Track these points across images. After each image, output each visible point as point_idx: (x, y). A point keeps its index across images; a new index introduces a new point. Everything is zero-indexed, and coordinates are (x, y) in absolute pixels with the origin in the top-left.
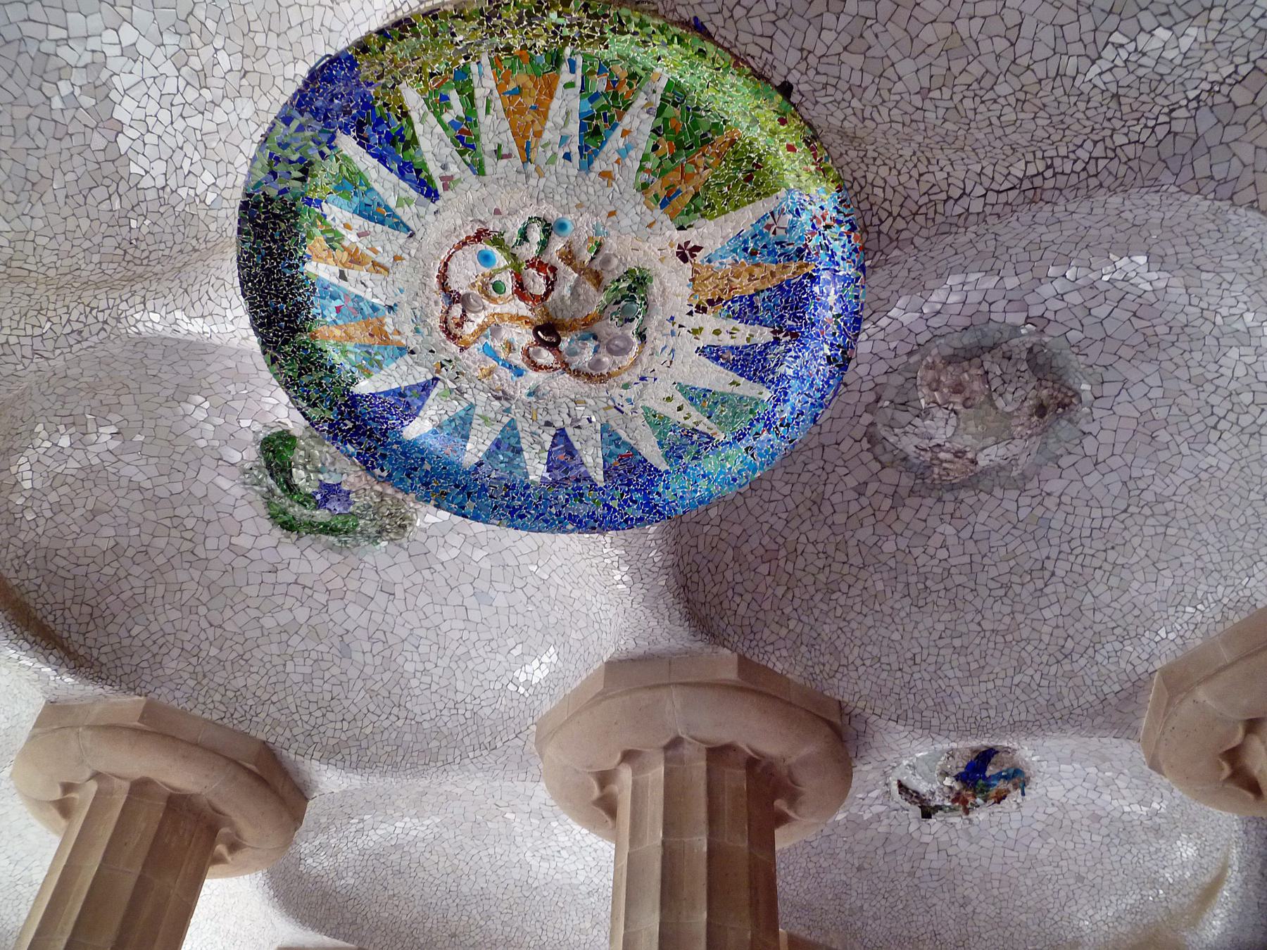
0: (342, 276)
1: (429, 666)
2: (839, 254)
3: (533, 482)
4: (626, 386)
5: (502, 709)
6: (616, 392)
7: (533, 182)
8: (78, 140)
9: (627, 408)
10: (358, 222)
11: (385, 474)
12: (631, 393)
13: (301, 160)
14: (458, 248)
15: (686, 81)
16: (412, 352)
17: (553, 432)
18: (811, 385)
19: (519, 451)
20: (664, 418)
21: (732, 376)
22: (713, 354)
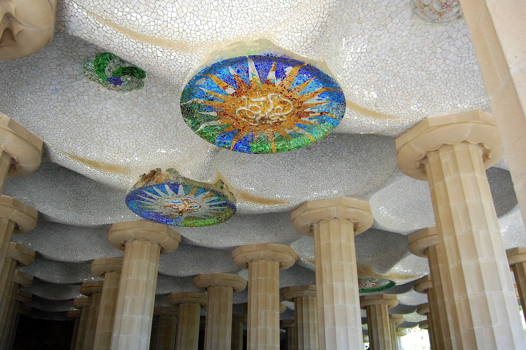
1: (24, 74)
5: (8, 100)
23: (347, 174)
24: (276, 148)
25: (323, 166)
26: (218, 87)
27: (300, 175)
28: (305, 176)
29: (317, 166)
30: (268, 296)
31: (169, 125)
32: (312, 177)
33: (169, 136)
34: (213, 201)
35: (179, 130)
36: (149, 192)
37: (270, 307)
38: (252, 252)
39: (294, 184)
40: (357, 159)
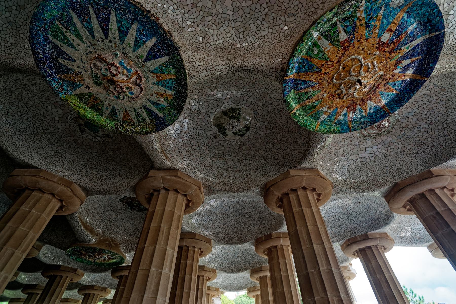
0: (165, 91)
2: (53, 83)
3: (113, 11)
4: (91, 52)
6: (93, 51)
7: (124, 106)
9: (89, 44)
10: (160, 103)
11: (160, 30)
12: (89, 50)
13: (169, 115)
14: (138, 96)
15: (100, 117)
16: (150, 71)
17: (109, 38)
18: (39, 44)
19: (119, 30)
20: (77, 37)
21: (63, 49)
22: (71, 59)
23: (216, 171)
26: (389, 23)
27: (190, 149)
28: (192, 152)
30: (29, 234)
31: (199, 9)
32: (195, 156)
33: (187, 15)
34: (156, 104)
35: (203, 23)
36: (118, 21)
38: (50, 182)
39: (181, 152)
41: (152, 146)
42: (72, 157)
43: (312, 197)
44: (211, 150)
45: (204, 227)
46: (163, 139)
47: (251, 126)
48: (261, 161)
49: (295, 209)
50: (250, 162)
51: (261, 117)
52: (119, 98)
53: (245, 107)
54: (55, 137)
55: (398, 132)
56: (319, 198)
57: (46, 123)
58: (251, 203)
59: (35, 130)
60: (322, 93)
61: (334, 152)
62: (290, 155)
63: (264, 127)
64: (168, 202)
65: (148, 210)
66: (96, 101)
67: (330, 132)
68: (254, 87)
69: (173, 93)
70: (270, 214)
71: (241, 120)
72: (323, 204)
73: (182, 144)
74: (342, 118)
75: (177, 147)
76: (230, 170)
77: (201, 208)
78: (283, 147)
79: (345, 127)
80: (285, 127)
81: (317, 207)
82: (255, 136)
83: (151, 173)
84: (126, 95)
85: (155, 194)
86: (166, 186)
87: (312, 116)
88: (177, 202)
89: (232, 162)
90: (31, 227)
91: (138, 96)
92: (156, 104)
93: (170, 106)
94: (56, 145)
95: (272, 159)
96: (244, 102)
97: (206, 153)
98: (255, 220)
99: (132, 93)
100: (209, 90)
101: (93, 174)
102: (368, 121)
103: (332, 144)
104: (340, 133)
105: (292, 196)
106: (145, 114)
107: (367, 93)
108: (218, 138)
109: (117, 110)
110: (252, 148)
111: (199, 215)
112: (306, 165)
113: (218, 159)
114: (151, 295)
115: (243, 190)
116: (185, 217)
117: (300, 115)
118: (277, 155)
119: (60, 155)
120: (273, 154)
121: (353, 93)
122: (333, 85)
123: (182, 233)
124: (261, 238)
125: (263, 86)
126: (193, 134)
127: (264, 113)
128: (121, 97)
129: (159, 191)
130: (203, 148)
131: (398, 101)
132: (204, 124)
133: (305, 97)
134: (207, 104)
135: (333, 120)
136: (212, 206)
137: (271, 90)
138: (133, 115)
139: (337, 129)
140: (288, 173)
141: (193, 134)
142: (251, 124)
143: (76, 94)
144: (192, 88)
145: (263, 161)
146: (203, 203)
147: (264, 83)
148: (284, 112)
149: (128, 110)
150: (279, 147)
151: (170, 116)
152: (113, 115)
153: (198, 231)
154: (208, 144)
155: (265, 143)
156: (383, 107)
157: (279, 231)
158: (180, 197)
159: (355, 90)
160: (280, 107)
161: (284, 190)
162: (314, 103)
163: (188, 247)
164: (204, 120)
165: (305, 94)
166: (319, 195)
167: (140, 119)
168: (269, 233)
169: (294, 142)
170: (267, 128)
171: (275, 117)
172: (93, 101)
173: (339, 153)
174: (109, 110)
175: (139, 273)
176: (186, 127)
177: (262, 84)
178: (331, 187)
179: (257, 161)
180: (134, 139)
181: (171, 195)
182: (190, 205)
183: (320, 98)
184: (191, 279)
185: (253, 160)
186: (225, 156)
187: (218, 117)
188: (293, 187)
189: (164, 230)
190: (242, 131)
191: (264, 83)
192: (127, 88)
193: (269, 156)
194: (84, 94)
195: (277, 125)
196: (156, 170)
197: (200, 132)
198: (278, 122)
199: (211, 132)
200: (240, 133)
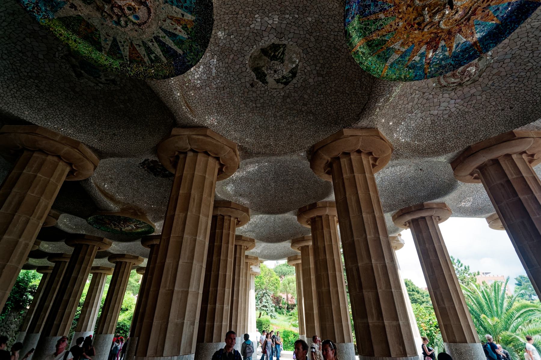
0: (183, 15)
7: (128, 38)
8: (293, 5)
10: (177, 33)
13: (191, 52)
14: (146, 22)
23: (253, 130)
24: (358, 49)
25: (243, 108)
27: (220, 101)
28: (223, 105)
29: (239, 105)
30: (41, 200)
34: (172, 35)
37: (37, 215)
38: (52, 142)
40: (274, 124)
41: (172, 95)
42: (72, 110)
43: (366, 161)
44: (247, 102)
45: (240, 195)
46: (185, 87)
47: (299, 71)
48: (309, 117)
49: (346, 175)
50: (296, 118)
51: (312, 58)
52: (120, 25)
53: (291, 43)
54: (44, 84)
55: (486, 81)
56: (376, 164)
57: (28, 63)
58: (295, 168)
59: (16, 73)
60: (397, 20)
61: (400, 107)
62: (345, 110)
63: (315, 72)
64: (197, 166)
65: (174, 175)
66: (89, 28)
67: (400, 79)
68: (304, 11)
69: (194, 18)
70: (316, 181)
71: (286, 62)
72: (378, 171)
73: (210, 95)
74: (417, 58)
75: (204, 98)
76: (271, 129)
77: (237, 174)
78: (337, 100)
79: (420, 73)
80: (342, 72)
81: (372, 173)
82: (303, 84)
83: (174, 131)
84: (129, 19)
85: (182, 156)
86: (194, 147)
87: (379, 56)
88: (208, 167)
89: (273, 119)
90: (42, 193)
91: (146, 22)
92: (172, 35)
93: (191, 39)
94: (48, 94)
95: (323, 115)
96: (291, 35)
97: (241, 106)
98: (298, 188)
99: (137, 18)
100: (243, 16)
101: (103, 132)
102: (451, 64)
103: (400, 96)
104: (412, 80)
105: (344, 161)
106: (159, 50)
107: (458, 23)
108: (256, 87)
109: (119, 44)
110: (298, 101)
111: (234, 182)
112: (363, 123)
113: (256, 114)
114: (186, 261)
115: (285, 153)
116: (218, 184)
117: (363, 54)
118: (328, 111)
119: (56, 107)
120: (325, 109)
121: (439, 22)
122: (413, 10)
123: (215, 201)
124: (305, 207)
125: (317, 10)
126: (223, 80)
127: (317, 52)
128: (123, 23)
129: (186, 153)
130: (237, 100)
131: (495, 36)
132: (237, 67)
133: (373, 28)
134: (241, 38)
135: (406, 63)
136: (249, 172)
137: (327, 17)
138: (142, 51)
139: (409, 74)
140: (341, 133)
141: (223, 80)
142: (299, 67)
143: (58, 18)
144: (219, 12)
145: (312, 118)
146: (239, 168)
147: (319, 5)
148: (343, 51)
149: (134, 43)
150: (333, 100)
151: (192, 54)
152: (114, 50)
153: (233, 199)
154: (243, 95)
155: (315, 95)
156: (475, 43)
157: (325, 200)
158: (211, 160)
159: (442, 18)
160: (338, 43)
161: (335, 154)
162: (384, 36)
163: (223, 216)
164: (237, 62)
165: (374, 23)
166: (375, 159)
167: (152, 56)
168: (314, 202)
169: (352, 94)
170: (319, 75)
171: (330, 59)
172: (85, 29)
173: (406, 109)
174: (110, 43)
175: (171, 240)
176: (214, 71)
177: (316, 7)
178: (390, 151)
179: (305, 118)
180: (149, 87)
181: (201, 158)
182: (224, 170)
183: (392, 29)
184: (228, 247)
185: (299, 116)
186: (264, 111)
187: (255, 57)
188: (346, 151)
189: (194, 197)
190: (286, 78)
191: (319, 5)
192: (129, 9)
193: (319, 111)
194: (70, 17)
195: (332, 70)
196: (179, 127)
197: (232, 79)
198: (334, 65)
199: (247, 79)
200: (285, 80)
